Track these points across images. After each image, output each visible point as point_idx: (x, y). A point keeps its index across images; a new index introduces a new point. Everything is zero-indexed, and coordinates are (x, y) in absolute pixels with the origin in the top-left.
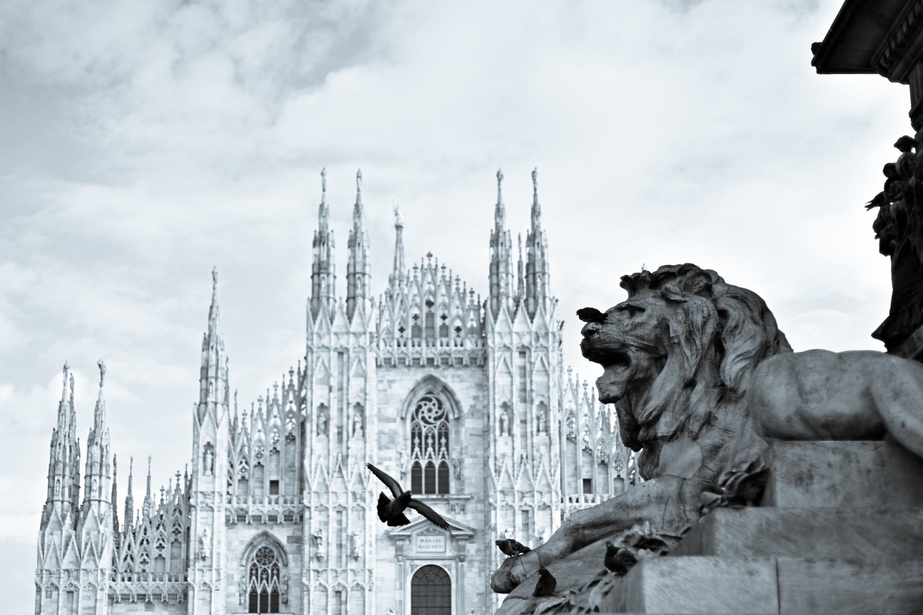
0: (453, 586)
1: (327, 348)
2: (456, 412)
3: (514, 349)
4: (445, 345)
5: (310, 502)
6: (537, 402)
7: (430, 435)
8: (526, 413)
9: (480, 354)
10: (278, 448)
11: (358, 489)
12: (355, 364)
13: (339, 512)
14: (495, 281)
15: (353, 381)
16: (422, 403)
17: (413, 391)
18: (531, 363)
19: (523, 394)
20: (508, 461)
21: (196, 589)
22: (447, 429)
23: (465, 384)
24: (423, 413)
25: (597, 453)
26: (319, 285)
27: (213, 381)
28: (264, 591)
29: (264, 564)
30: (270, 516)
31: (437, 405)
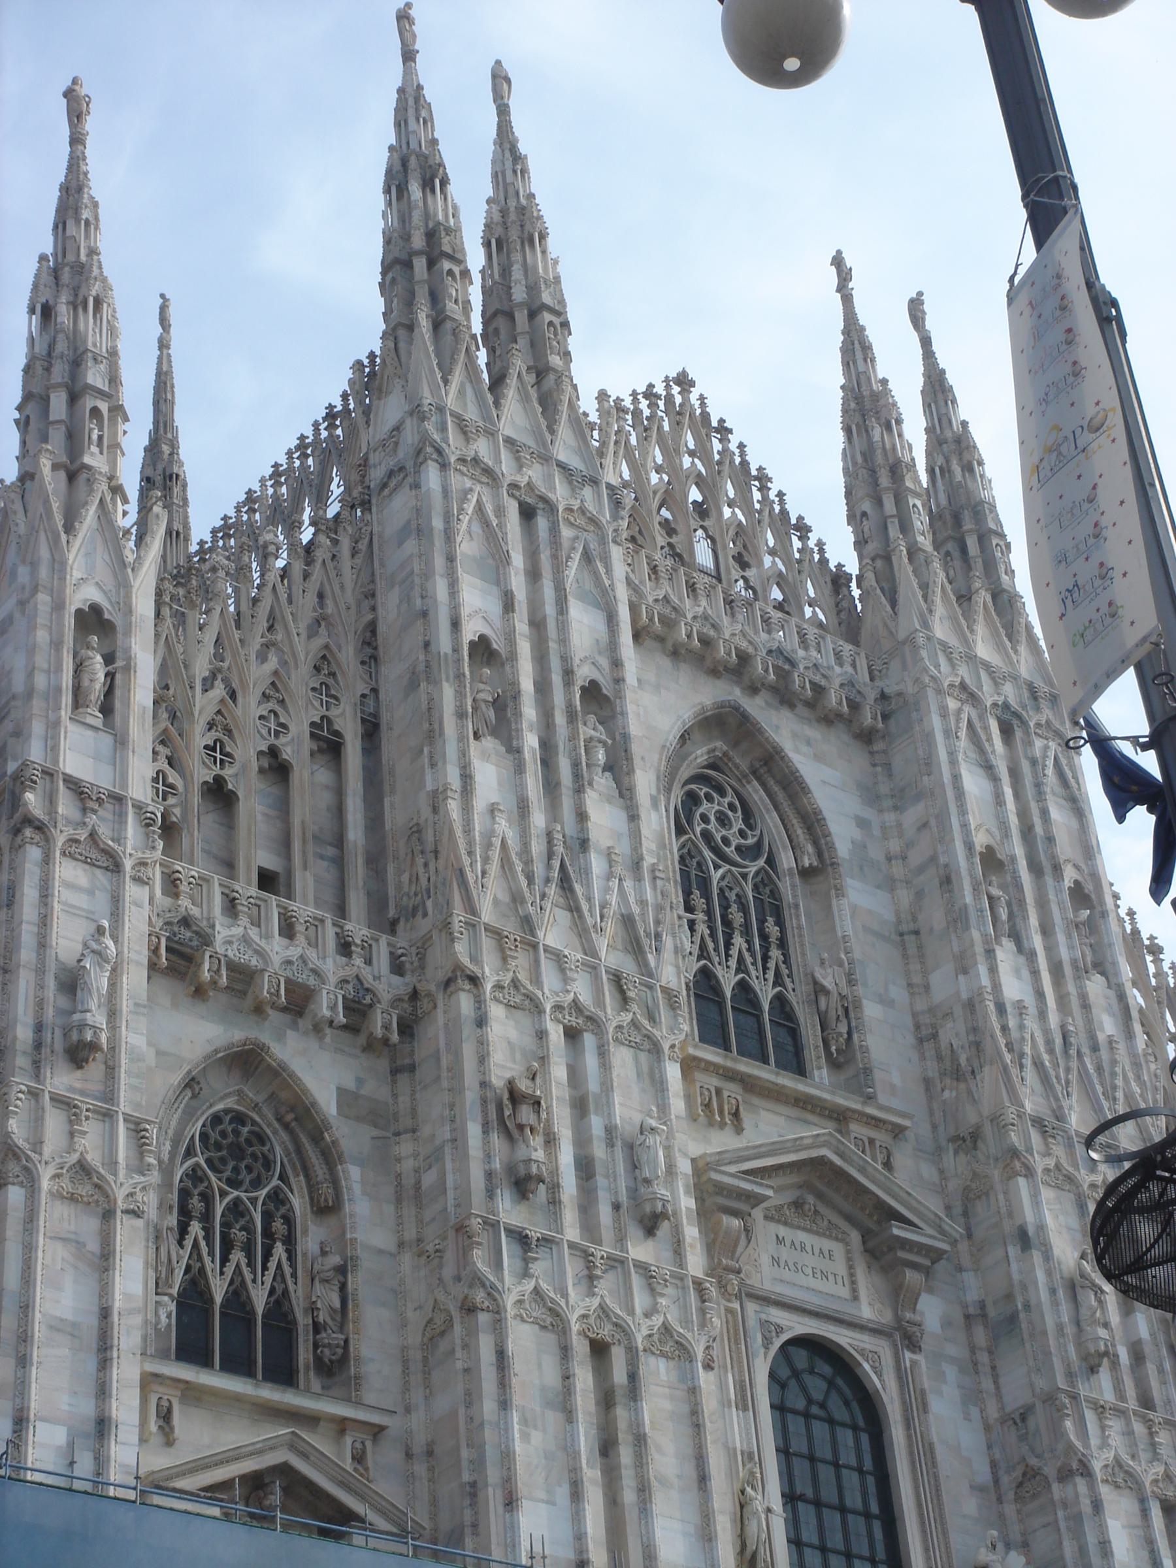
0: (897, 1435)
1: (487, 471)
2: (810, 848)
5: (474, 959)
6: (1068, 883)
7: (732, 896)
9: (871, 695)
10: (287, 753)
12: (577, 556)
13: (572, 1035)
14: (889, 506)
16: (702, 790)
18: (1034, 762)
20: (1032, 1024)
21: (45, 1184)
22: (775, 894)
24: (705, 819)
27: (104, 407)
28: (238, 1296)
29: (234, 1183)
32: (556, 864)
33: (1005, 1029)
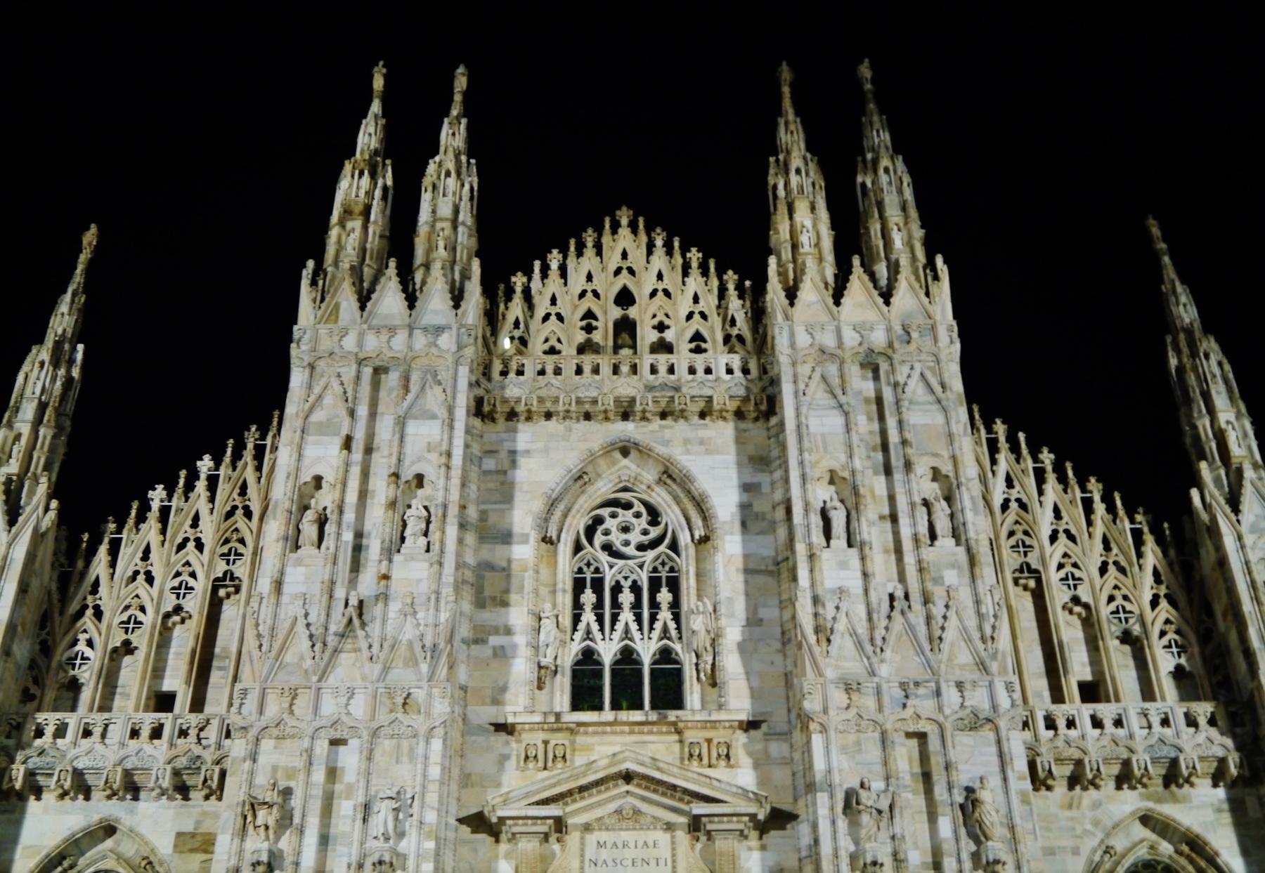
2: (697, 522)
3: (847, 355)
4: (663, 369)
8: (892, 499)
11: (401, 676)
15: (412, 428)
16: (605, 512)
17: (581, 478)
18: (896, 385)
19: (879, 456)
23: (718, 457)
24: (607, 533)
25: (1105, 611)
26: (340, 248)
30: (128, 774)
31: (645, 517)
32: (345, 621)
33: (816, 615)
